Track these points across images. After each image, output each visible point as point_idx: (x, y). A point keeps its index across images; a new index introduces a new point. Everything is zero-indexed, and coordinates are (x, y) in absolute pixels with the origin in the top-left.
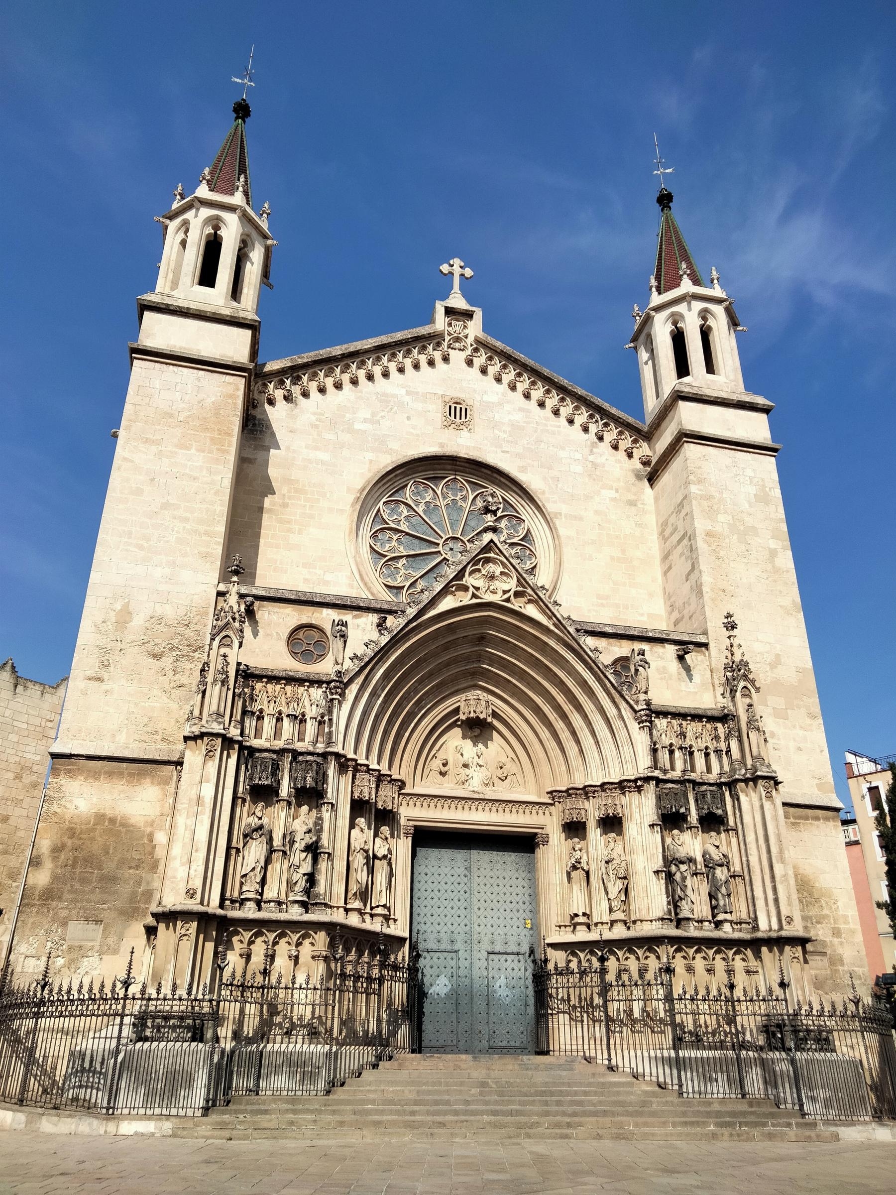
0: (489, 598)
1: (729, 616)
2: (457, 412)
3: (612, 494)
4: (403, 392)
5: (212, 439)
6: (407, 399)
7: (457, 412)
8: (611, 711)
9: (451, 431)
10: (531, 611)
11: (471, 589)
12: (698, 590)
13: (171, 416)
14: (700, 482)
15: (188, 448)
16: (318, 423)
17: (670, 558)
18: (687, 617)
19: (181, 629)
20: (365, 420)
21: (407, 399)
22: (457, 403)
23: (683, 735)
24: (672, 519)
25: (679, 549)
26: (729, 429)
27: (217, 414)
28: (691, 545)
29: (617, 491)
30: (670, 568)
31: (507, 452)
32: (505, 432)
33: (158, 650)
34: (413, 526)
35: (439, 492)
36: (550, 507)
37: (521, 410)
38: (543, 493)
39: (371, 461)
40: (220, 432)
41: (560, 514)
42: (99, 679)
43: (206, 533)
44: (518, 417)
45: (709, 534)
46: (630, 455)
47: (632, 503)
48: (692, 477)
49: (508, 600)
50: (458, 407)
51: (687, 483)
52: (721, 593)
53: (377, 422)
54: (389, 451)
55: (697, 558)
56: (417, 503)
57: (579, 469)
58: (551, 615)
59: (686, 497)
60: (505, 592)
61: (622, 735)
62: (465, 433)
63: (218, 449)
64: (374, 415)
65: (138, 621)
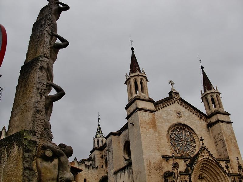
0: (206, 157)
1: (237, 158)
2: (179, 114)
5: (154, 127)
7: (179, 114)
8: (224, 175)
10: (211, 159)
12: (226, 151)
13: (146, 122)
14: (223, 130)
15: (150, 129)
18: (223, 155)
19: (158, 165)
20: (165, 117)
23: (234, 179)
30: (217, 145)
33: (156, 169)
37: (188, 113)
40: (154, 125)
42: (150, 175)
43: (157, 146)
45: (226, 140)
46: (206, 122)
47: (208, 132)
49: (208, 157)
51: (221, 130)
54: (170, 123)
58: (214, 159)
59: (221, 132)
60: (207, 155)
61: (226, 179)
65: (152, 164)
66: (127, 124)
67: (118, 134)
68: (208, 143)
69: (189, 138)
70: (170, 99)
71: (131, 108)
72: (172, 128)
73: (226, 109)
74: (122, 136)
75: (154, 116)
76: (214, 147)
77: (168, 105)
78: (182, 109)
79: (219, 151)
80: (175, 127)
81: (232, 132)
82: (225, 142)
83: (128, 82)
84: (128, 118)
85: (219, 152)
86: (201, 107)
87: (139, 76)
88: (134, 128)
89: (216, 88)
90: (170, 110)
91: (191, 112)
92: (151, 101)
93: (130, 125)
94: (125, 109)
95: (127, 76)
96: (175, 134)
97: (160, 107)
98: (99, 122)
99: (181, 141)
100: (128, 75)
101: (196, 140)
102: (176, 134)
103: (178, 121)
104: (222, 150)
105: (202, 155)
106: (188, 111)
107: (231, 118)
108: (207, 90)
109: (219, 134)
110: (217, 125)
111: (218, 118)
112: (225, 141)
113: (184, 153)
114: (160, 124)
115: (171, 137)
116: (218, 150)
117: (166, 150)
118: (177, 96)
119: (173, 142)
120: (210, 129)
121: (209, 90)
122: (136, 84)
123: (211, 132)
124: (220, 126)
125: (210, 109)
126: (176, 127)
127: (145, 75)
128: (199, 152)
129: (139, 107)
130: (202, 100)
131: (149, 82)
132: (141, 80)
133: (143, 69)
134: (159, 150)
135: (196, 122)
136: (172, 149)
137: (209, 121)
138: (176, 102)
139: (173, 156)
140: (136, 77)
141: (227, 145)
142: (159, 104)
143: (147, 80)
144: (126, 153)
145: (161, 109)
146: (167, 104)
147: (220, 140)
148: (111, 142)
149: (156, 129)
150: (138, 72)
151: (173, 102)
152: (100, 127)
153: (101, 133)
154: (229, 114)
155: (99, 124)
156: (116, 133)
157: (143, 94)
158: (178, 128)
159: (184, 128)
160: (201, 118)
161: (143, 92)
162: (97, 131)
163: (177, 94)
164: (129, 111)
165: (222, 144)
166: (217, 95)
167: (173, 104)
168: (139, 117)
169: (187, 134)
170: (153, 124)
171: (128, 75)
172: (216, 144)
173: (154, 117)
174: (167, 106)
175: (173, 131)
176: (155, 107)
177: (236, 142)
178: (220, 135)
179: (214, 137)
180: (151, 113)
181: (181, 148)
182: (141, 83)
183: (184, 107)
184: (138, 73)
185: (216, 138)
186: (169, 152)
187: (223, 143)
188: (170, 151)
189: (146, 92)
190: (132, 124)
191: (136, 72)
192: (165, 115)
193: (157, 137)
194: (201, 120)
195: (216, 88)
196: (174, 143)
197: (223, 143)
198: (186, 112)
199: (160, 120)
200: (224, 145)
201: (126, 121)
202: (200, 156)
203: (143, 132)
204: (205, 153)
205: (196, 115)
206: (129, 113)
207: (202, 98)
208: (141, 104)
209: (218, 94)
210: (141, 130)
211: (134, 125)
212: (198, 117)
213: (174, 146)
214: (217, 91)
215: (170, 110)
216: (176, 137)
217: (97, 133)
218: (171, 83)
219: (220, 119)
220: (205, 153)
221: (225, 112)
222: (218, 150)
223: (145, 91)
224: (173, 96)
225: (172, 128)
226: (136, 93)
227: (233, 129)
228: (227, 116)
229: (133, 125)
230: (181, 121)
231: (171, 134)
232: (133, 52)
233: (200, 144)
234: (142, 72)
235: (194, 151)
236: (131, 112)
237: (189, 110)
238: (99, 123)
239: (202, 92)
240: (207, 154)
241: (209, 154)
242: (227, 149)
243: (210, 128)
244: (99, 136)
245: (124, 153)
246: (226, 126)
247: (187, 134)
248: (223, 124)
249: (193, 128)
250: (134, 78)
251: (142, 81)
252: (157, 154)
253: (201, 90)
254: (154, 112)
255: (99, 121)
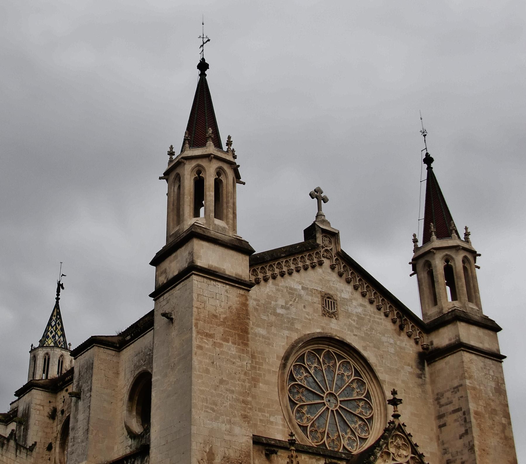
2: (329, 305)
3: (409, 369)
4: (300, 287)
5: (239, 335)
6: (303, 292)
7: (329, 305)
9: (326, 319)
11: (392, 454)
12: (471, 448)
13: (215, 316)
14: (470, 377)
16: (257, 307)
17: (445, 418)
20: (282, 307)
21: (303, 292)
22: (328, 298)
24: (448, 395)
25: (455, 416)
26: (481, 343)
27: (239, 317)
28: (465, 419)
29: (412, 368)
30: (444, 425)
31: (356, 335)
32: (354, 320)
34: (308, 382)
35: (321, 360)
36: (381, 376)
37: (361, 305)
38: (376, 366)
39: (287, 337)
41: (385, 381)
43: (243, 402)
44: (360, 310)
45: (476, 413)
46: (417, 343)
47: (419, 376)
48: (466, 375)
50: (330, 300)
51: (463, 377)
52: (483, 451)
53: (288, 309)
54: (297, 330)
55: (471, 428)
56: (310, 367)
57: (392, 350)
59: (461, 385)
60: (406, 457)
62: (334, 320)
63: (242, 343)
64: (286, 303)
66: (153, 312)
67: (118, 343)
68: (413, 417)
69: (353, 389)
70: (308, 250)
71: (171, 262)
72: (301, 348)
73: (489, 310)
74: (129, 353)
75: (247, 300)
76: (432, 430)
77: (298, 271)
78: (343, 291)
79: (446, 446)
80: (310, 348)
81: (500, 390)
82: (473, 420)
83: (172, 176)
84: (156, 295)
85: (445, 451)
86: (406, 290)
87: (214, 161)
88: (174, 333)
89: (467, 234)
90: (303, 288)
91: (371, 302)
92: (241, 247)
93: (159, 321)
94: (152, 263)
95: (171, 153)
96: (307, 371)
97: (269, 274)
98: (58, 295)
99: (325, 396)
100: (177, 151)
101: (376, 401)
102: (312, 371)
103: (323, 328)
104: (460, 443)
105: (388, 454)
106: (361, 300)
107: (504, 343)
108: (434, 237)
109: (456, 389)
110: (451, 360)
111: (458, 336)
112: (472, 415)
113: (328, 437)
114: (262, 331)
115: (292, 378)
116: (443, 443)
117: (272, 419)
118: (330, 242)
119: (297, 397)
120: (427, 368)
121: (440, 236)
122: (199, 184)
123: (428, 380)
124: (463, 362)
125: (435, 301)
126: (316, 347)
127: (235, 157)
128: (379, 440)
129: (200, 263)
130: (414, 269)
131: (244, 184)
132: (218, 174)
133: (229, 137)
134: (245, 417)
135: (384, 339)
136: (290, 420)
137: (426, 340)
138: (327, 263)
139: (292, 442)
140: (204, 163)
141: (476, 432)
142: (267, 262)
143: (237, 176)
144: (134, 413)
145: (271, 281)
146: (293, 267)
147: (455, 411)
148: (90, 367)
149: (246, 345)
150: (210, 143)
151: (315, 260)
152: (59, 313)
153: (59, 333)
154: (496, 329)
155: (57, 302)
156: (109, 339)
157: (217, 222)
158: (319, 351)
159: (344, 355)
160: (401, 328)
161: (218, 214)
162: (49, 324)
163: (333, 236)
164: (165, 272)
165: (461, 425)
166: (465, 257)
167: (313, 267)
168: (195, 296)
169: (348, 376)
170: (239, 327)
171: (177, 151)
172: (441, 423)
173: (245, 305)
174: (295, 274)
175: (301, 358)
176: (254, 271)
177: (510, 423)
178: (459, 394)
179: (437, 400)
180: (235, 289)
181: (322, 420)
182: (218, 183)
183: (348, 282)
184: (210, 149)
185: (443, 401)
186: (281, 427)
187: (465, 421)
188: (283, 425)
189: (231, 216)
190: (167, 318)
191: (202, 144)
192: (281, 302)
193: (245, 374)
194: (400, 335)
195: (467, 234)
196: (301, 400)
197: (465, 421)
198: (355, 303)
199: (265, 318)
200: (466, 432)
201: (149, 305)
202: (382, 456)
203: (200, 347)
204: (398, 447)
205: (386, 315)
206: (163, 280)
207: (414, 263)
208: (207, 255)
209: (470, 257)
210: (195, 343)
211: (176, 323)
212: (394, 322)
213: (298, 411)
214: (466, 245)
215: (303, 288)
216: (311, 379)
217: (47, 331)
218: (317, 195)
219: (464, 339)
220: (398, 447)
221: (486, 318)
222: (443, 443)
223: (225, 211)
224: (319, 241)
225: (301, 348)
226: (197, 214)
227: (503, 379)
228: (491, 333)
229: (171, 320)
230: (335, 328)
231: (295, 369)
232: (203, 75)
233: (386, 416)
234: (225, 148)
235: (363, 435)
236: (171, 276)
237: (363, 295)
238: (58, 299)
239: (415, 241)
240: (405, 453)
241: (413, 453)
242: (476, 443)
243: (428, 365)
244: (52, 344)
245: (130, 411)
246: (481, 364)
247: (348, 376)
248: (473, 357)
249: (372, 359)
250: (194, 163)
251: (222, 178)
252: (237, 430)
253: (414, 235)
254: (245, 285)
255: (58, 291)
